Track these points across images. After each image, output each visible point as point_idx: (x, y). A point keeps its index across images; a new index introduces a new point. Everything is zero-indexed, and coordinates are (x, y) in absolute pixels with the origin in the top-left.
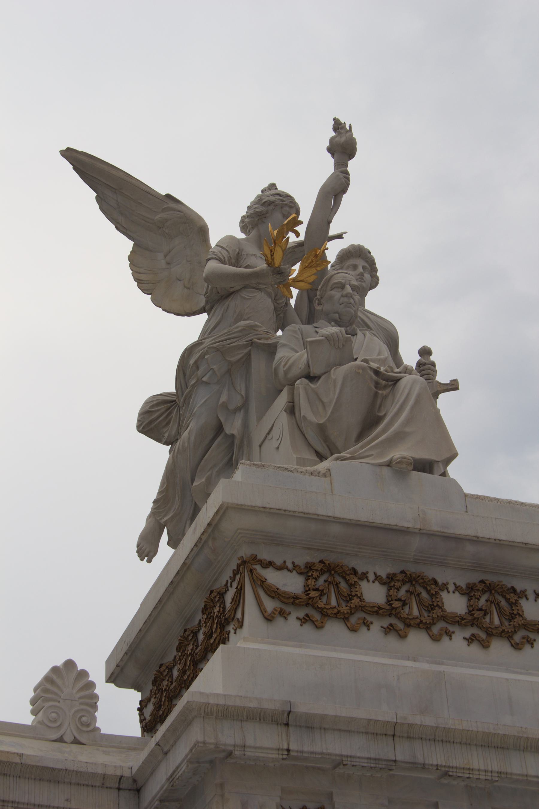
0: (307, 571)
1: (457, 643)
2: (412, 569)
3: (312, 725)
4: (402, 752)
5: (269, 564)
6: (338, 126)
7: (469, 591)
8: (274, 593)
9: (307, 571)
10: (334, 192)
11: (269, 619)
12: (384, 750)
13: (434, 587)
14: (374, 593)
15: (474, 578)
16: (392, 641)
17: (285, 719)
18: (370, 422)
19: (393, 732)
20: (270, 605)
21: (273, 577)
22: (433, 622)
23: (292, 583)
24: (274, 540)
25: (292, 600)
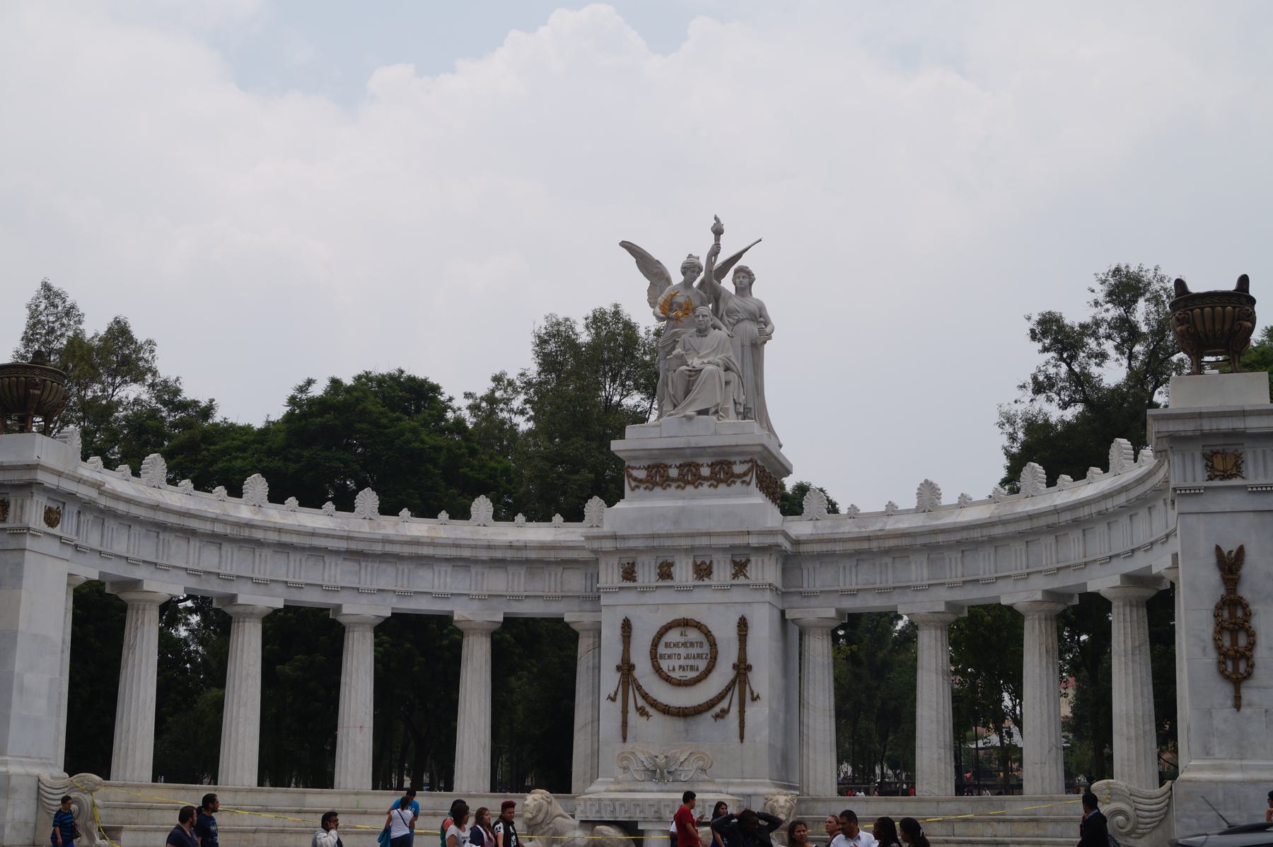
0: (648, 468)
1: (705, 488)
2: (690, 460)
3: (624, 538)
4: (656, 543)
5: (633, 468)
6: (716, 218)
7: (712, 466)
8: (635, 479)
9: (648, 468)
10: (715, 251)
11: (633, 490)
12: (650, 543)
13: (698, 466)
14: (673, 473)
15: (714, 460)
16: (679, 492)
17: (615, 537)
18: (687, 392)
19: (653, 536)
20: (633, 484)
21: (635, 473)
22: (697, 480)
23: (641, 474)
24: (635, 458)
25: (641, 481)
